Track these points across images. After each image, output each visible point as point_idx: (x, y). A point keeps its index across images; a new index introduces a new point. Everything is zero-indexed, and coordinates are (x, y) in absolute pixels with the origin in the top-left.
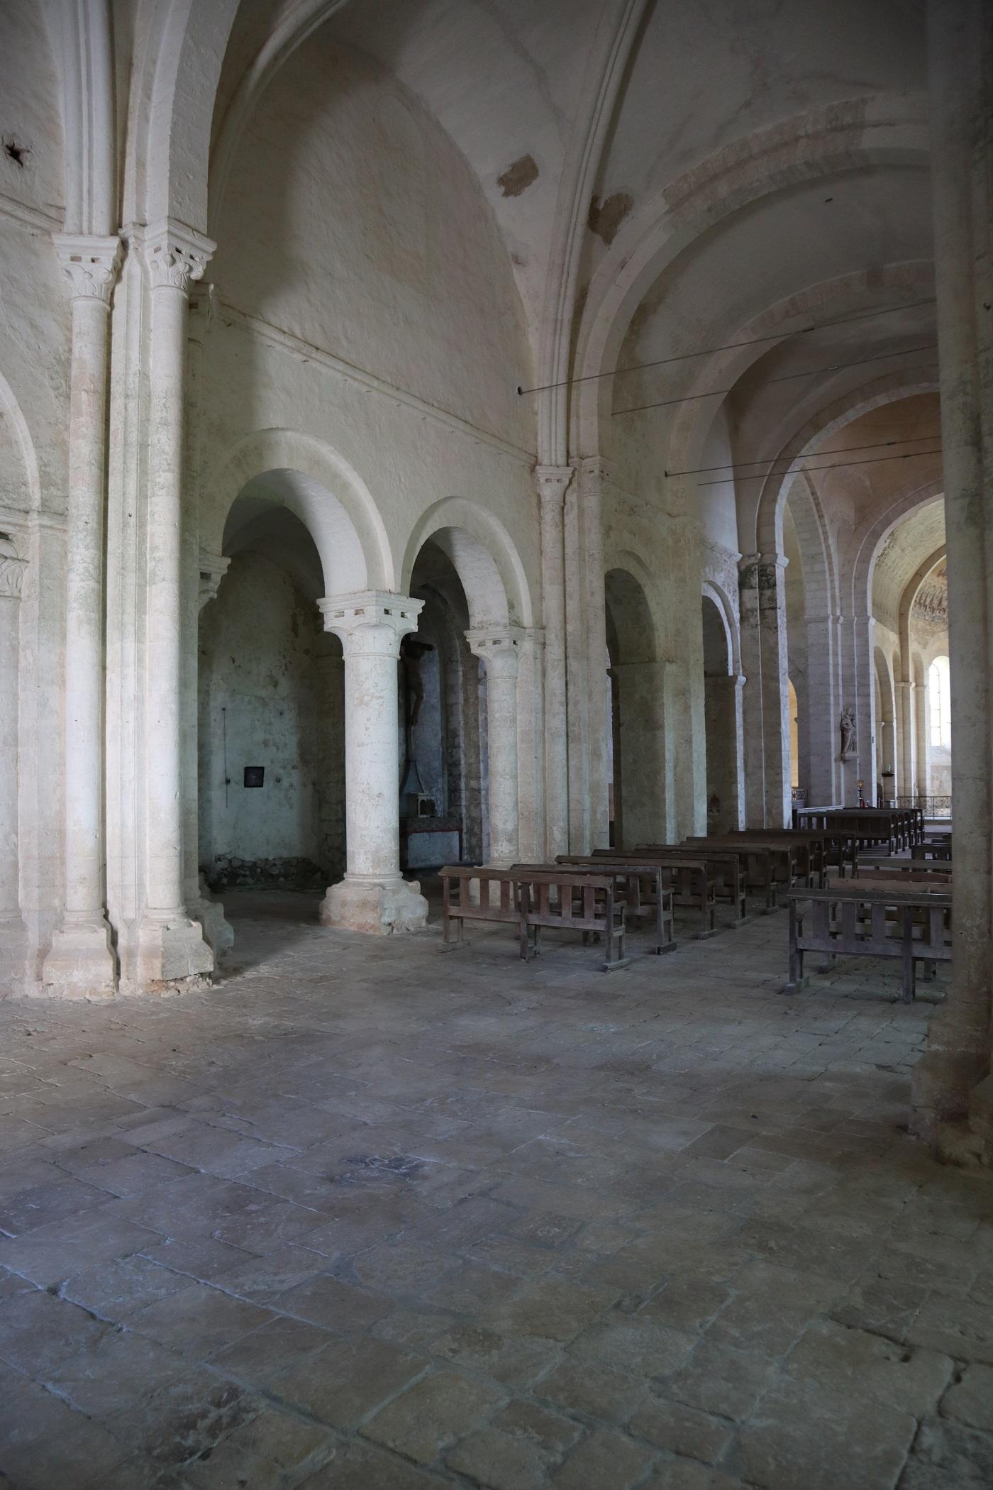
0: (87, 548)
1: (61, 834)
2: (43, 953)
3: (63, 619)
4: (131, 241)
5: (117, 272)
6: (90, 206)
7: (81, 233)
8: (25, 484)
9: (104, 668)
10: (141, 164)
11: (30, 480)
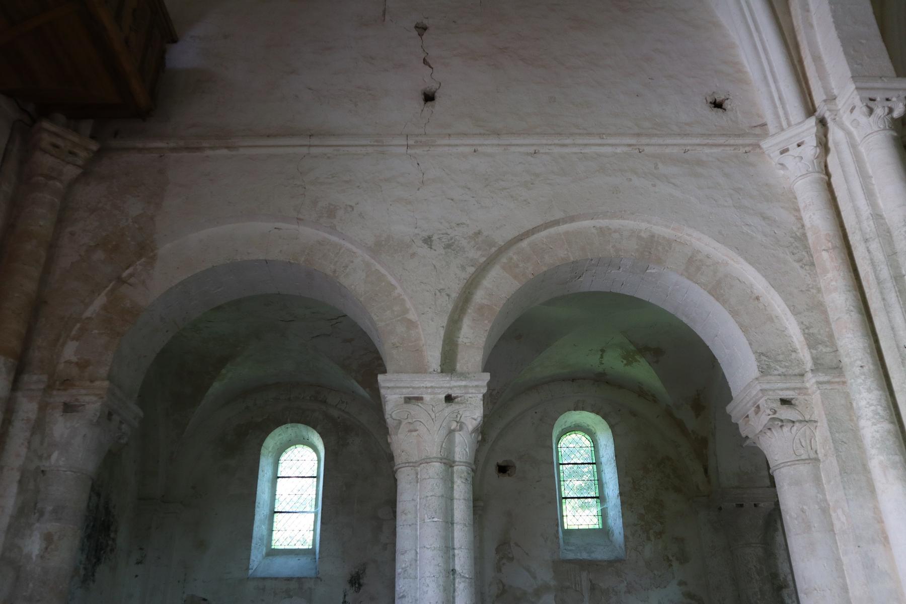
0: (869, 390)
3: (866, 470)
4: (828, 116)
5: (824, 145)
6: (784, 108)
7: (783, 130)
8: (795, 351)
10: (817, 59)
11: (798, 347)
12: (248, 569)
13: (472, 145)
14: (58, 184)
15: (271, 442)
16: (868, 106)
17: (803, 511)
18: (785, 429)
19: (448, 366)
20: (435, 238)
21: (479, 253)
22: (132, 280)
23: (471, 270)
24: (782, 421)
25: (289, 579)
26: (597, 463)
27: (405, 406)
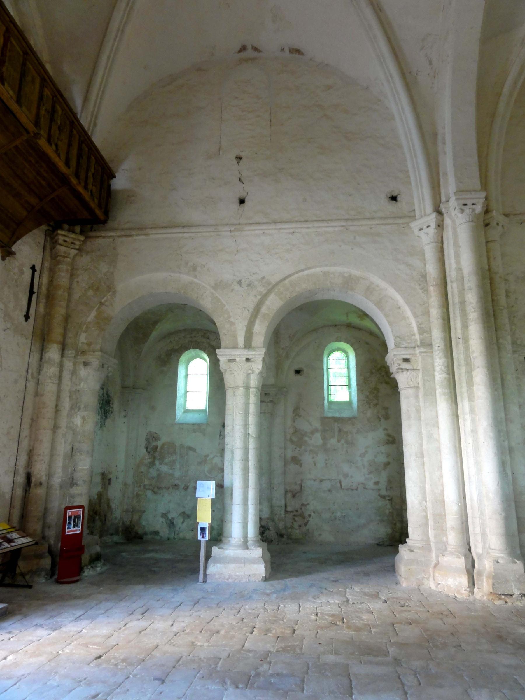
0: (440, 358)
1: (443, 502)
2: (436, 565)
4: (444, 211)
5: (440, 226)
8: (414, 335)
9: (457, 416)
10: (445, 174)
12: (175, 419)
13: (261, 230)
14: (68, 259)
15: (184, 358)
16: (461, 209)
17: (408, 410)
18: (404, 373)
19: (248, 345)
20: (243, 281)
21: (263, 288)
22: (106, 304)
23: (259, 297)
24: (402, 369)
25: (194, 424)
26: (348, 368)
27: (229, 363)
